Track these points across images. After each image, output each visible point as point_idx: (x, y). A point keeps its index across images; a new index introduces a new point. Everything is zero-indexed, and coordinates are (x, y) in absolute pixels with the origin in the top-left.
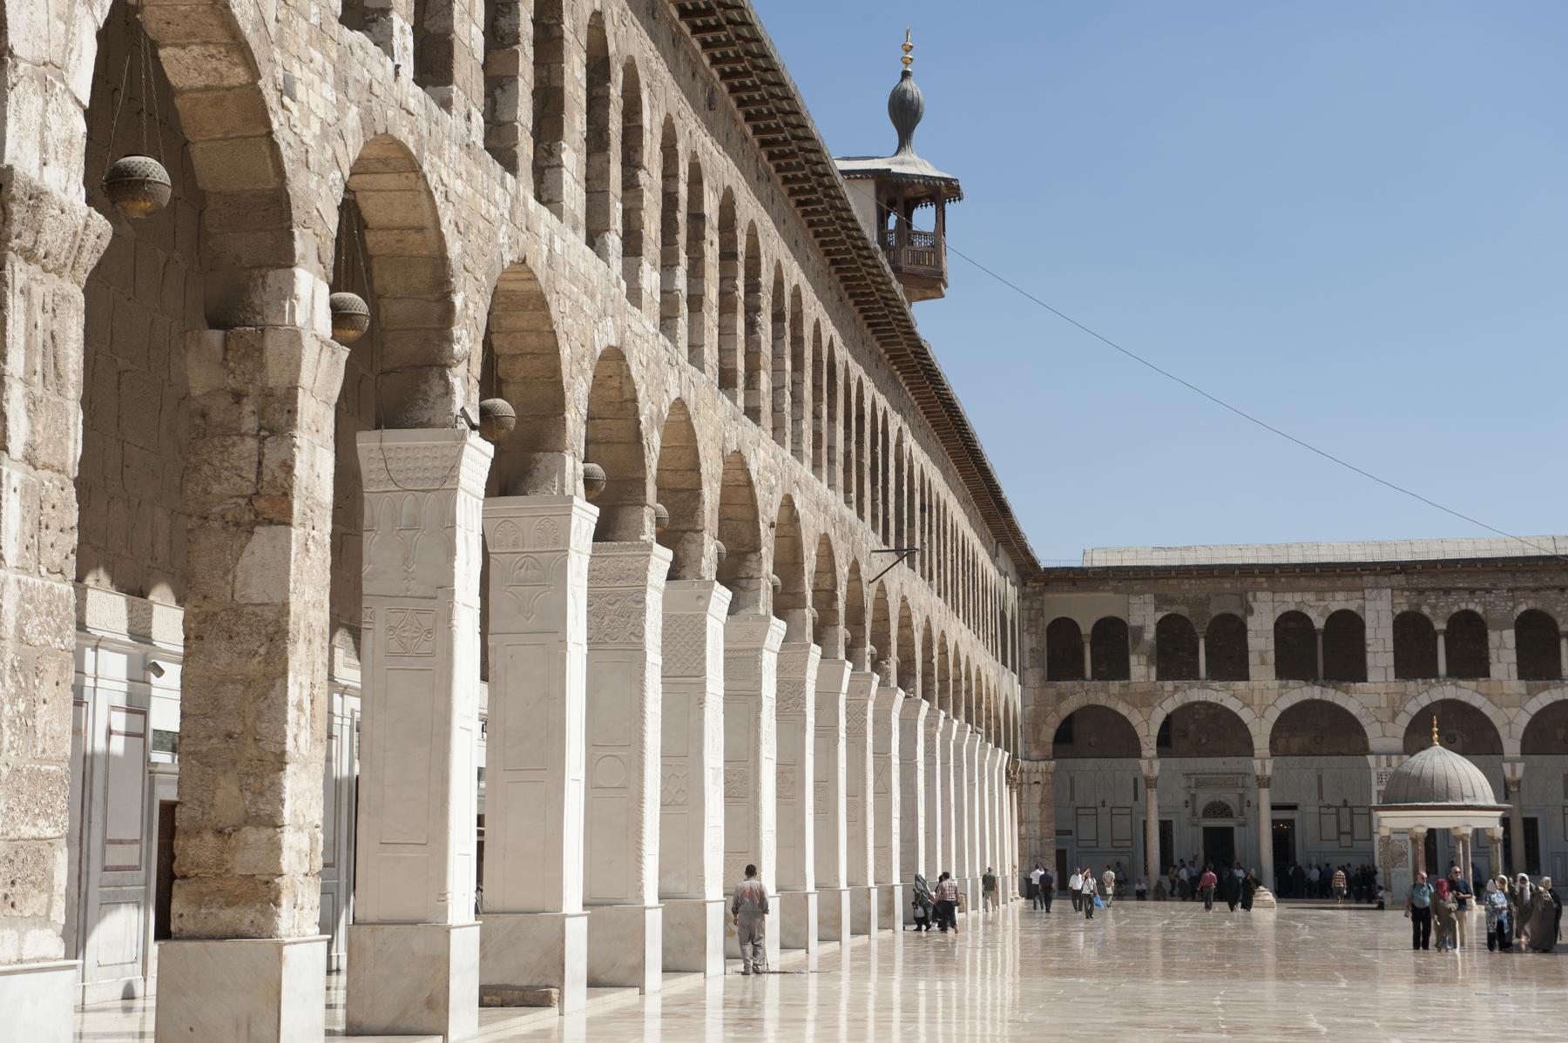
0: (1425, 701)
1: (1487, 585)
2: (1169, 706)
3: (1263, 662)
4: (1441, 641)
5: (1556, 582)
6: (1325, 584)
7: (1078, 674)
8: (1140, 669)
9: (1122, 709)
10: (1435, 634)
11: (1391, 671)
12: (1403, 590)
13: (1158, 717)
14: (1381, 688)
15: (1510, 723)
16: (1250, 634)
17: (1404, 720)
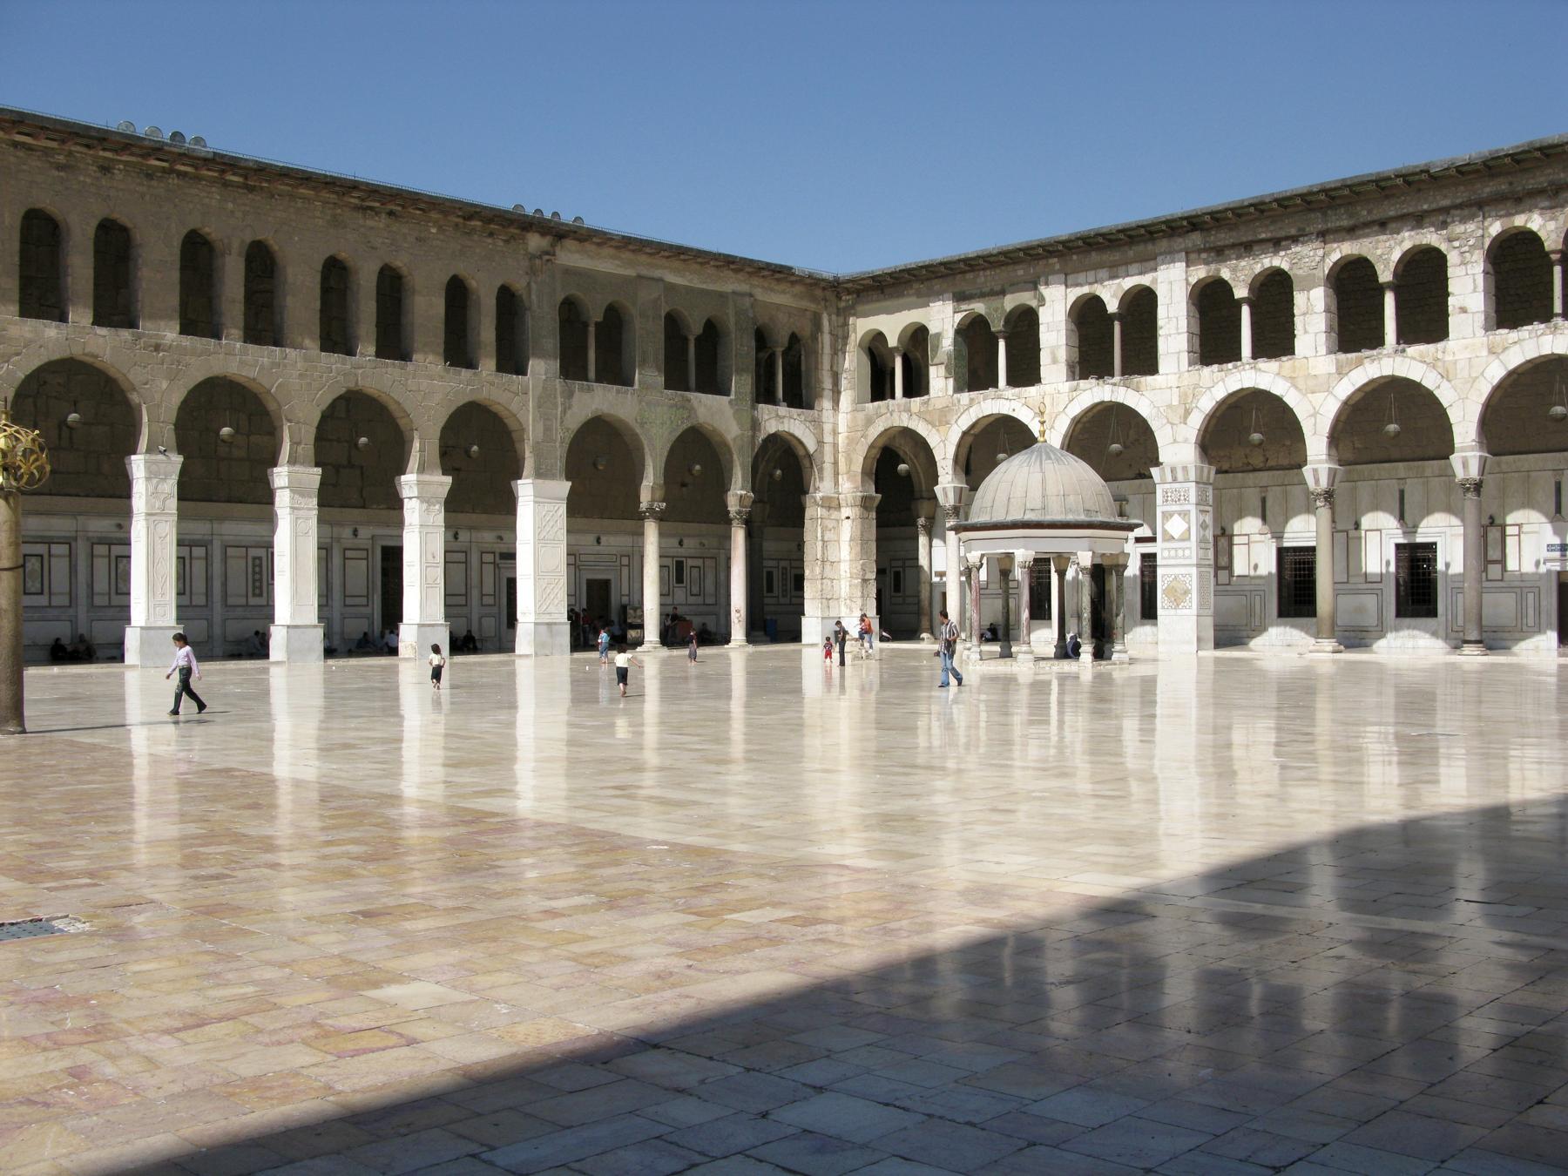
0: (1220, 393)
1: (1293, 232)
2: (965, 422)
3: (1055, 361)
5: (1377, 214)
6: (1116, 256)
8: (939, 380)
9: (922, 429)
10: (1238, 304)
11: (1185, 357)
12: (1200, 251)
14: (1173, 381)
15: (1314, 415)
16: (1042, 328)
17: (1197, 420)
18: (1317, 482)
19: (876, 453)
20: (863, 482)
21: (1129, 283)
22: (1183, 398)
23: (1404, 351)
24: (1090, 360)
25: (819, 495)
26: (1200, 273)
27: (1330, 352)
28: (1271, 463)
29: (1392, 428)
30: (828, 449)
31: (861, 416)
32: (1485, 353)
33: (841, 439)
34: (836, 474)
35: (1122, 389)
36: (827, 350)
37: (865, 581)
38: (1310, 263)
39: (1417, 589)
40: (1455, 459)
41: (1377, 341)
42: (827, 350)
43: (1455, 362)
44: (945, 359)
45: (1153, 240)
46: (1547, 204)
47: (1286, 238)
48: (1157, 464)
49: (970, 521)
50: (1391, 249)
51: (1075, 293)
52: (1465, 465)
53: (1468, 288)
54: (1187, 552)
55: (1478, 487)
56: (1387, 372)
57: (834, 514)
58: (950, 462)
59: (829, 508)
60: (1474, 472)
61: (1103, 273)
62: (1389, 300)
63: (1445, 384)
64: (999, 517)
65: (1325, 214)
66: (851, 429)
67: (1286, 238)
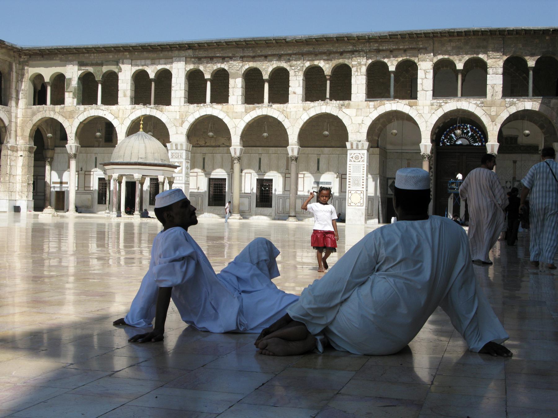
0: (197, 115)
1: (230, 55)
2: (82, 118)
3: (125, 96)
4: (209, 84)
5: (264, 53)
6: (155, 55)
7: (45, 103)
8: (70, 99)
9: (60, 119)
10: (206, 81)
11: (183, 100)
12: (191, 58)
13: (76, 123)
14: (177, 109)
15: (236, 127)
16: (120, 81)
18: (235, 153)
19: (35, 128)
20: (29, 140)
21: (160, 67)
22: (181, 116)
23: (271, 106)
24: (140, 96)
25: (9, 145)
26: (191, 67)
27: (243, 104)
28: (207, 144)
29: (264, 135)
30: (13, 125)
31: (29, 111)
32: (302, 110)
33: (19, 121)
34: (16, 136)
35: (155, 110)
36: (14, 80)
37: (29, 184)
38: (237, 68)
39: (264, 197)
40: (289, 148)
41: (261, 101)
42: (14, 80)
43: (291, 112)
44: (73, 90)
45: (172, 51)
46: (325, 58)
47: (228, 57)
48: (169, 142)
49: (112, 161)
50: (268, 66)
51: (135, 69)
52: (293, 151)
53: (296, 85)
54: (181, 178)
55: (296, 159)
56: (265, 113)
57: (15, 154)
58: (74, 135)
59: (13, 151)
60: (296, 154)
61: (148, 62)
62: (266, 86)
63: (286, 120)
64: (127, 160)
65: (243, 50)
66: (24, 116)
67: (228, 57)
